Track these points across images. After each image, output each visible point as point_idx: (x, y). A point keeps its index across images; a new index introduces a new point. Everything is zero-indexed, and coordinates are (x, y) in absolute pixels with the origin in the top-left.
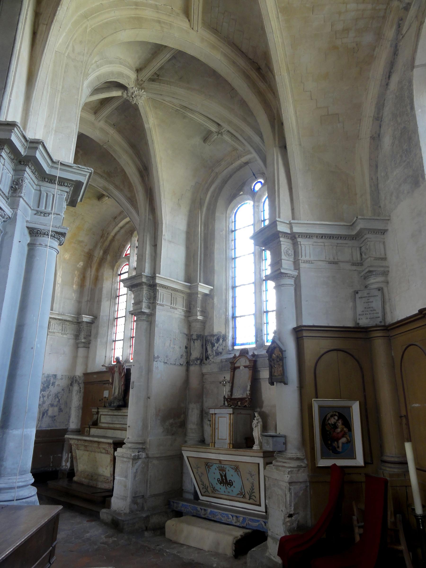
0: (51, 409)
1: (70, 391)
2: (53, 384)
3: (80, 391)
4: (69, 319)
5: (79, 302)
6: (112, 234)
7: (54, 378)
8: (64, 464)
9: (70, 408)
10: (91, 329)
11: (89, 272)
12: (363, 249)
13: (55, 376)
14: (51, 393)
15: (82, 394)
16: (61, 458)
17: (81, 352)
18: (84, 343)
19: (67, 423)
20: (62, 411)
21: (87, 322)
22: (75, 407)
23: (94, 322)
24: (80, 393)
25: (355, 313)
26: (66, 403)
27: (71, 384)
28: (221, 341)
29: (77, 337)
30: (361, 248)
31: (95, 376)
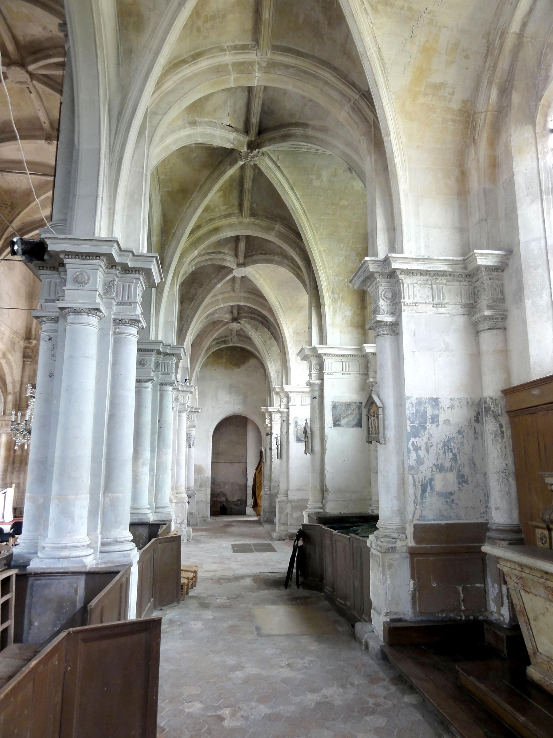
0: (439, 478)
1: (478, 435)
2: (434, 419)
3: (502, 432)
4: (443, 268)
5: (462, 230)
6: (515, 27)
7: (433, 407)
8: (493, 607)
9: (485, 474)
10: (502, 285)
11: (472, 155)
13: (435, 401)
14: (433, 441)
15: (508, 440)
16: (484, 593)
17: (489, 340)
18: (490, 318)
19: (483, 510)
20: (466, 482)
21: (489, 268)
22: (497, 473)
23: (507, 265)
24: (503, 437)
26: (473, 463)
27: (478, 418)
29: (471, 308)
31: (536, 392)
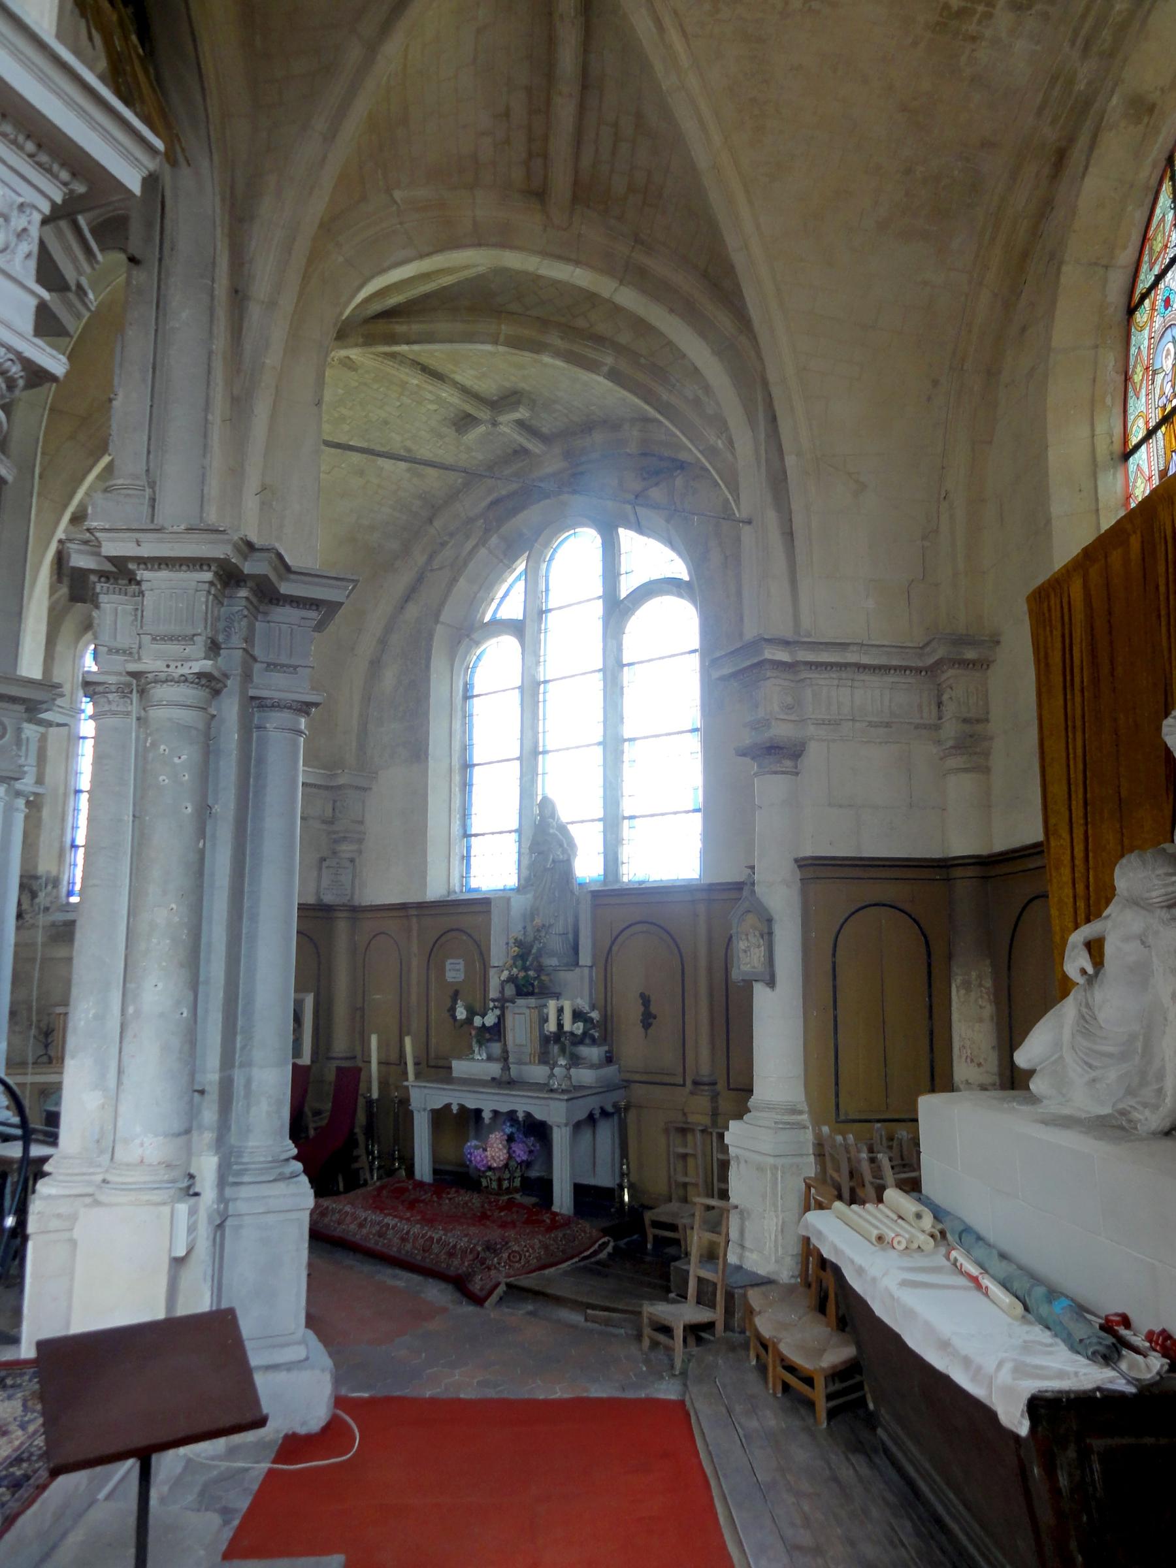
12: (338, 803)
25: (319, 886)
28: (49, 888)
30: (335, 801)
